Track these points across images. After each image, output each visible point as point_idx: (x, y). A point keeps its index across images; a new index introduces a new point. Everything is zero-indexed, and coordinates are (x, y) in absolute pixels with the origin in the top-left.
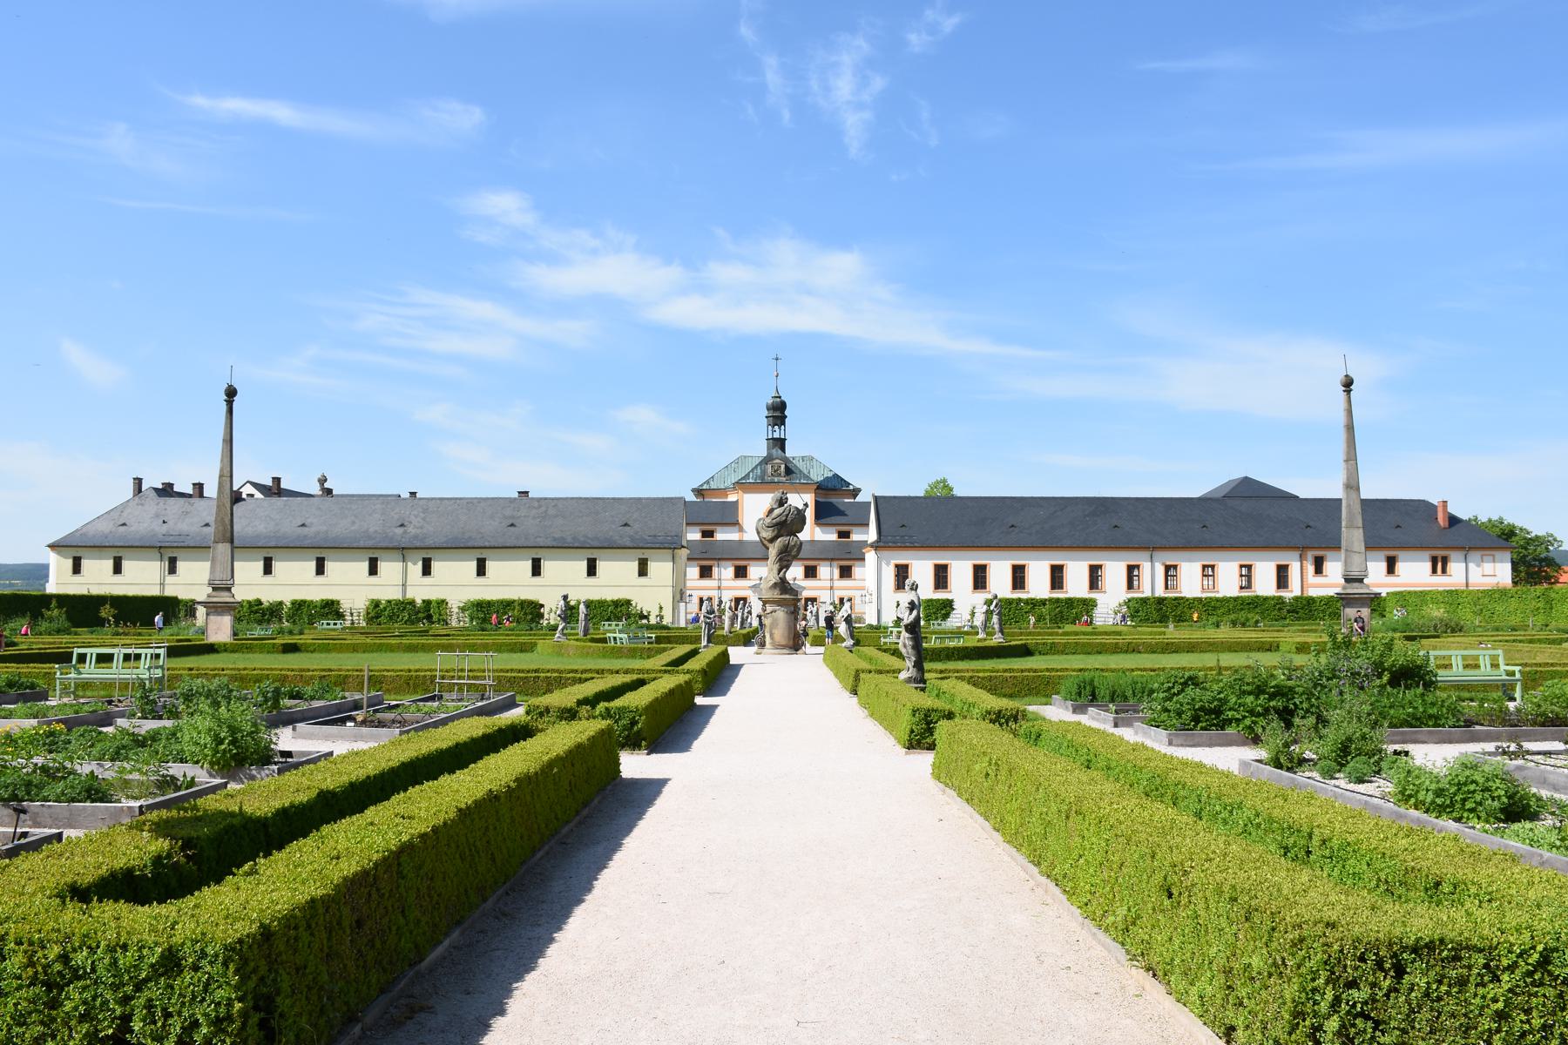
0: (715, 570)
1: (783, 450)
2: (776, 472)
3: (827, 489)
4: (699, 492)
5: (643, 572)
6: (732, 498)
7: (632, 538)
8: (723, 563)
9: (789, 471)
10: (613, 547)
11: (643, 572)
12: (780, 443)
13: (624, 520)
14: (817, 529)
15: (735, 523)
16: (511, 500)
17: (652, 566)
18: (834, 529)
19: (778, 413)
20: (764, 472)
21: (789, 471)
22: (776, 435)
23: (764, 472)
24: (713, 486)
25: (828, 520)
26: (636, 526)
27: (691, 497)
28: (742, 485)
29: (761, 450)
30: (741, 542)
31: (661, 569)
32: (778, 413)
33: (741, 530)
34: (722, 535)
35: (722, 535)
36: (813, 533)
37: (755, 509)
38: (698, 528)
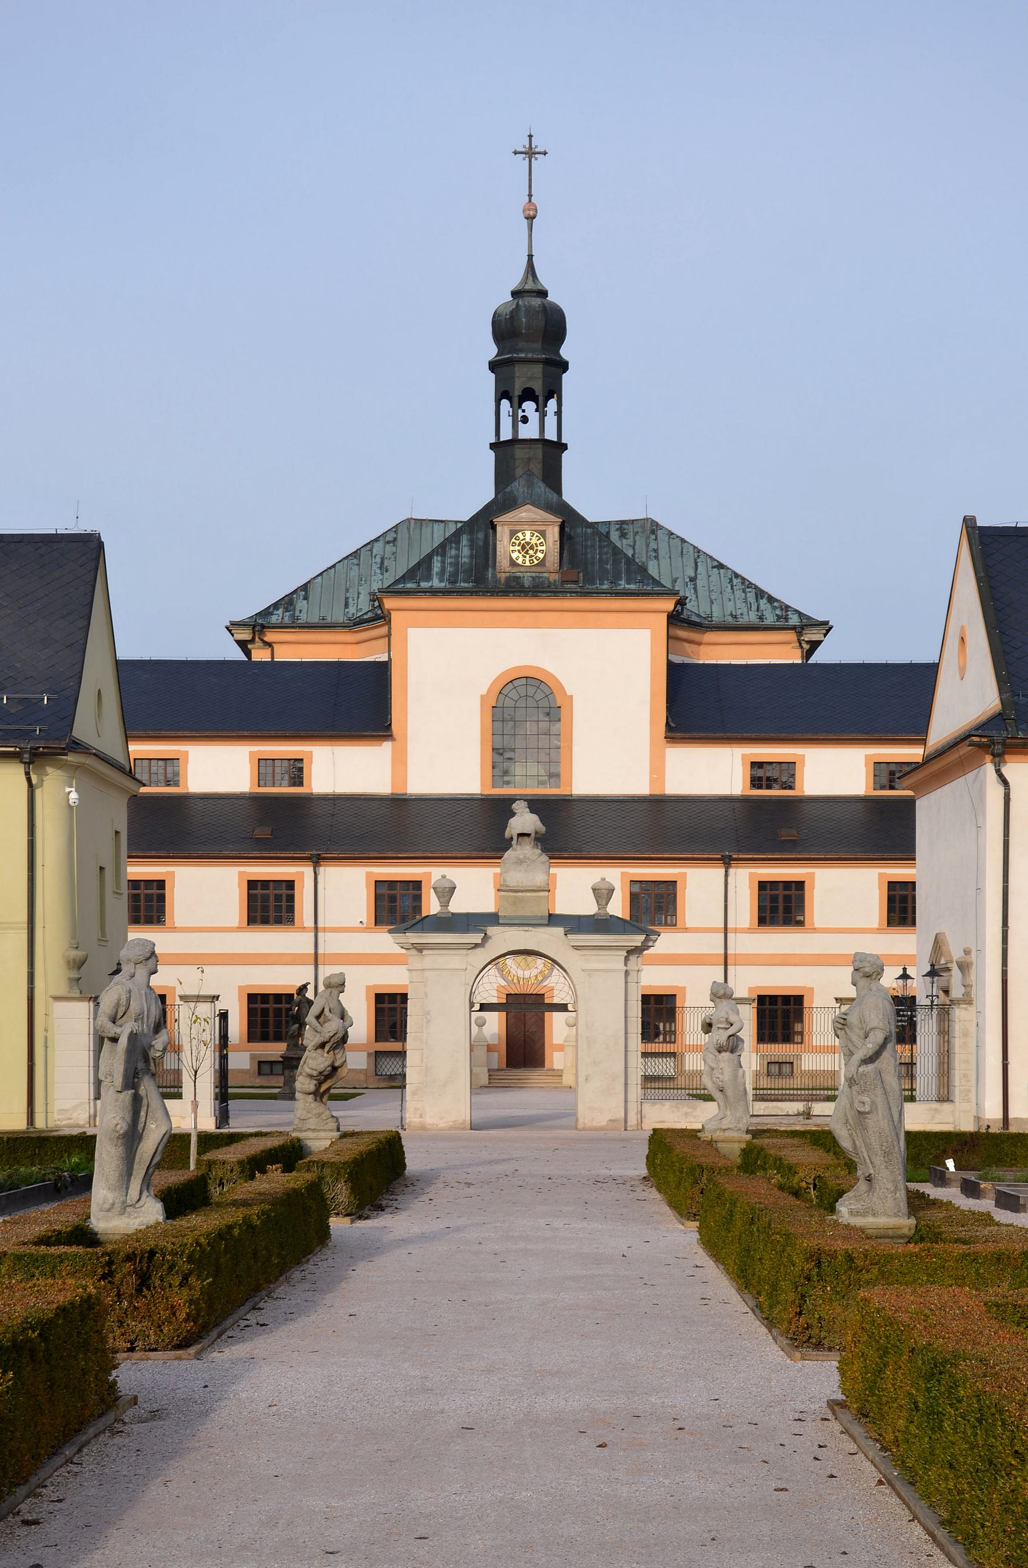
1: (553, 477)
22: (529, 431)
36: (657, 769)
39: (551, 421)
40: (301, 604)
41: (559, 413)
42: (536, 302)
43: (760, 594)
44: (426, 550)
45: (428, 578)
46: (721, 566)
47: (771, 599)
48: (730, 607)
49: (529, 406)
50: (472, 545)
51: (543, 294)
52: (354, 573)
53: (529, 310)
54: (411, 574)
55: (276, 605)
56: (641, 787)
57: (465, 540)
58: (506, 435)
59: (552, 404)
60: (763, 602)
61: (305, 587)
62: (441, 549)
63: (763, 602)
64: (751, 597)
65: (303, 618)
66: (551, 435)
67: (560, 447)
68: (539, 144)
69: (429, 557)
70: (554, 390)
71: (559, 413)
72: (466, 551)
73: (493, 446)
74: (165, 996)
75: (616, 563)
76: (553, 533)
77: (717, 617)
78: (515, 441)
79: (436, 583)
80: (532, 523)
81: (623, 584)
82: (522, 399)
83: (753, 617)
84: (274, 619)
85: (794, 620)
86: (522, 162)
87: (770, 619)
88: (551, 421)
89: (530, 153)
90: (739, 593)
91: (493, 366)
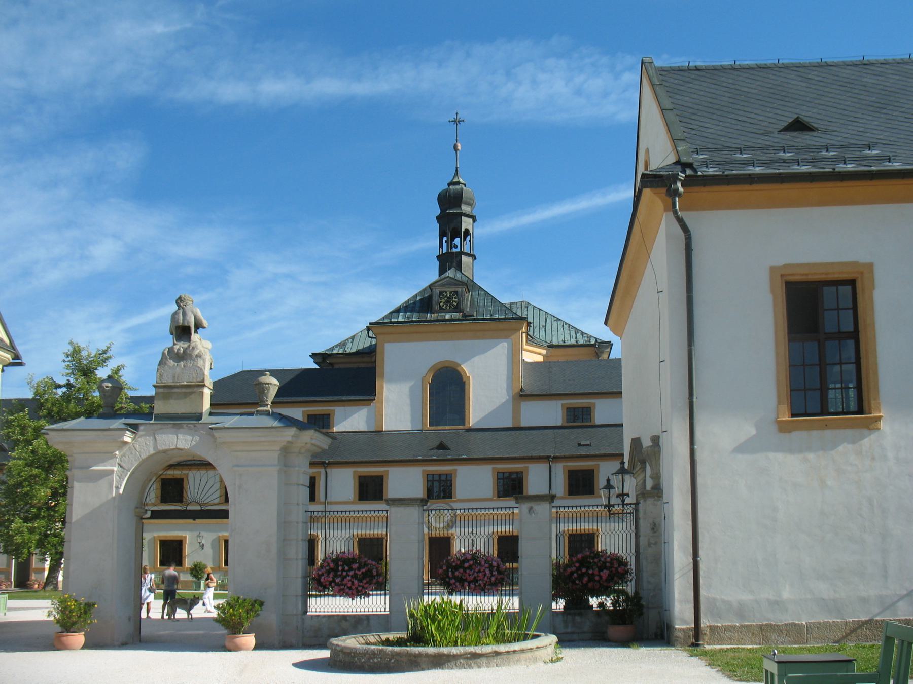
27: (312, 365)
36: (516, 413)
40: (349, 345)
43: (577, 331)
46: (558, 320)
47: (583, 333)
48: (561, 338)
55: (336, 346)
61: (353, 338)
63: (579, 335)
65: (348, 351)
77: (555, 342)
81: (496, 316)
83: (573, 342)
84: (334, 352)
85: (593, 342)
87: (581, 342)
90: (567, 332)
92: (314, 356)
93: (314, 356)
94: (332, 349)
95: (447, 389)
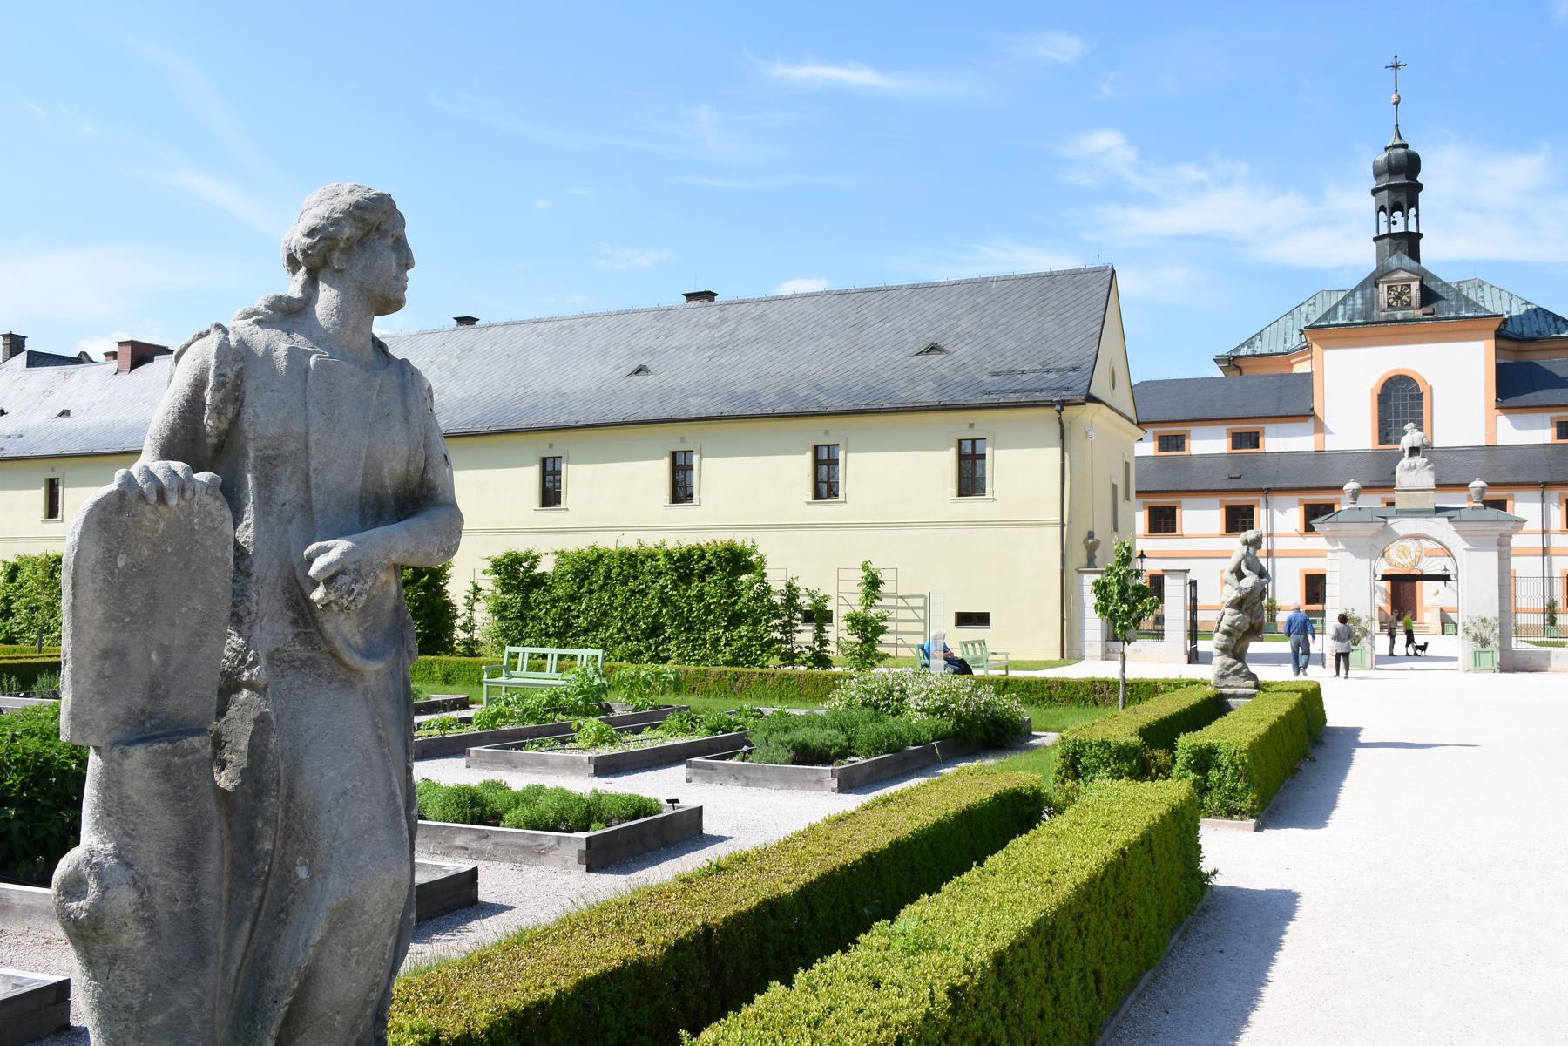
0: (1260, 515)
1: (1414, 254)
2: (1399, 298)
3: (1521, 339)
4: (1231, 362)
5: (970, 481)
6: (1301, 368)
7: (942, 383)
8: (1276, 499)
9: (1429, 296)
10: (883, 411)
11: (970, 481)
12: (1410, 243)
13: (930, 337)
14: (1503, 421)
15: (1306, 415)
16: (662, 313)
17: (1001, 464)
18: (1546, 417)
19: (1401, 181)
20: (1370, 303)
21: (1429, 296)
22: (1397, 229)
23: (1370, 303)
24: (1261, 348)
25: (1530, 398)
26: (962, 352)
28: (1324, 332)
29: (1365, 257)
30: (1319, 454)
31: (1025, 470)
32: (1401, 181)
33: (1320, 427)
34: (1276, 442)
35: (1276, 442)
36: (1491, 428)
37: (1347, 384)
38: (1222, 429)
39: (1412, 221)
40: (1258, 343)
41: (1417, 216)
42: (1402, 151)
44: (1334, 302)
45: (1336, 318)
48: (1535, 327)
49: (1397, 214)
50: (1363, 296)
51: (1405, 146)
52: (1290, 324)
53: (1397, 155)
54: (1325, 317)
56: (1481, 441)
57: (1358, 294)
58: (1383, 231)
59: (1412, 211)
60: (1559, 323)
61: (1260, 334)
62: (1344, 301)
64: (1550, 320)
66: (1412, 229)
67: (1419, 236)
68: (1401, 60)
69: (1336, 306)
70: (1414, 203)
71: (1417, 216)
72: (1359, 301)
73: (1375, 239)
74: (818, 495)
75: (1458, 301)
76: (1415, 286)
78: (1389, 235)
79: (1340, 321)
80: (1402, 280)
81: (1463, 314)
82: (1392, 210)
86: (1391, 72)
88: (1412, 221)
89: (1396, 66)
90: (1541, 319)
91: (1374, 192)
92: (1218, 360)
93: (1218, 360)
94: (1237, 349)
95: (1400, 401)
